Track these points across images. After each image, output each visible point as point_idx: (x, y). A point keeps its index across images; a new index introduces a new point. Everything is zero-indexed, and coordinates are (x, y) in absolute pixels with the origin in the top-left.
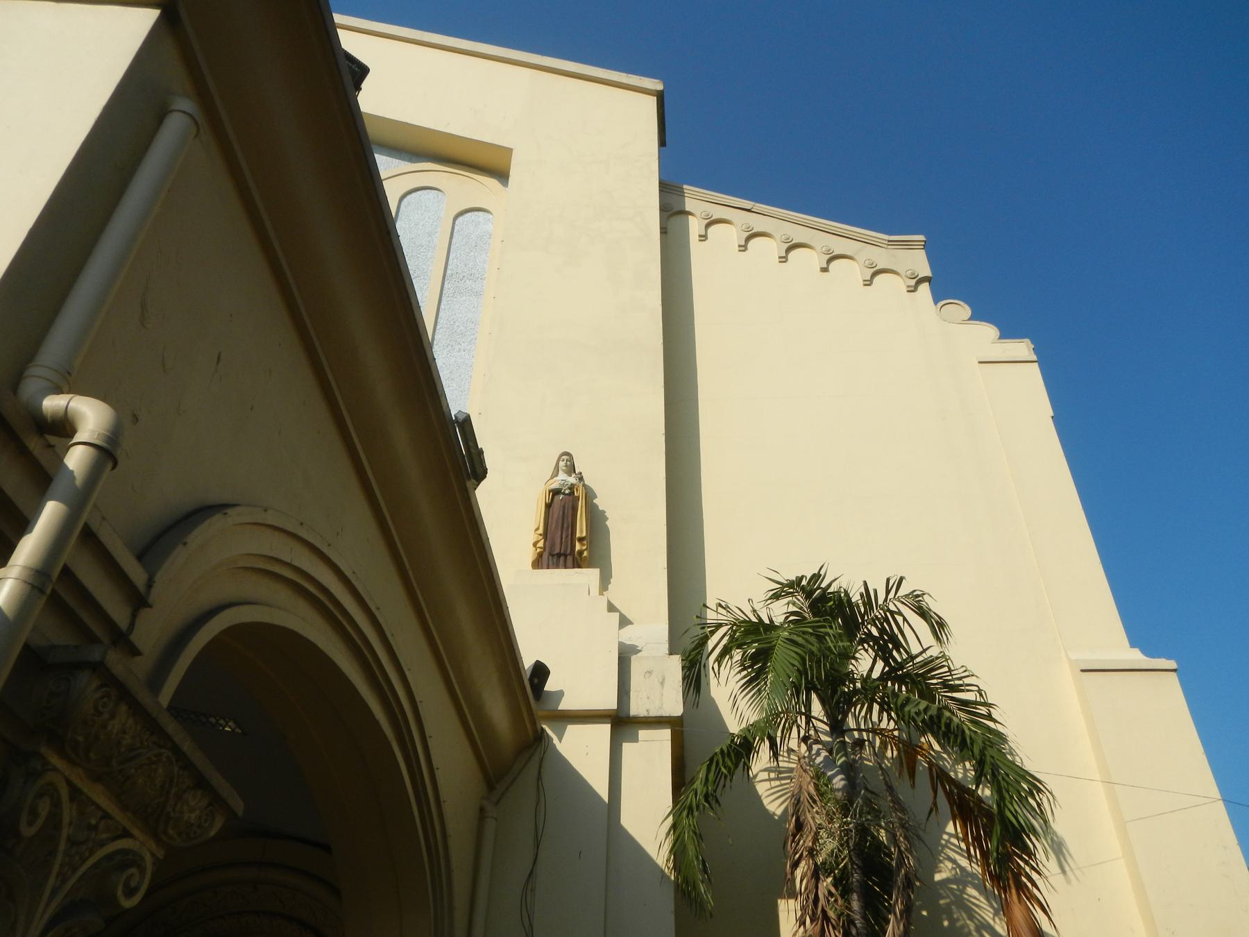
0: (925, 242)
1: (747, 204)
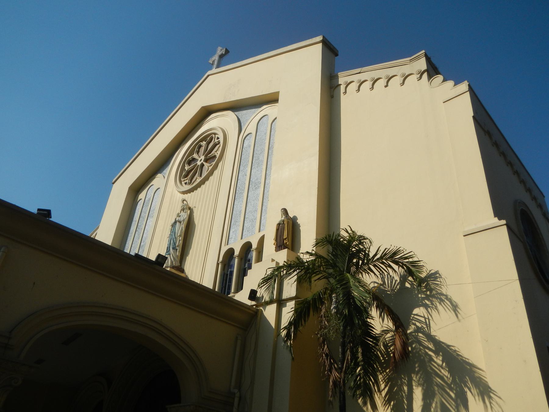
0: (425, 53)
1: (358, 70)
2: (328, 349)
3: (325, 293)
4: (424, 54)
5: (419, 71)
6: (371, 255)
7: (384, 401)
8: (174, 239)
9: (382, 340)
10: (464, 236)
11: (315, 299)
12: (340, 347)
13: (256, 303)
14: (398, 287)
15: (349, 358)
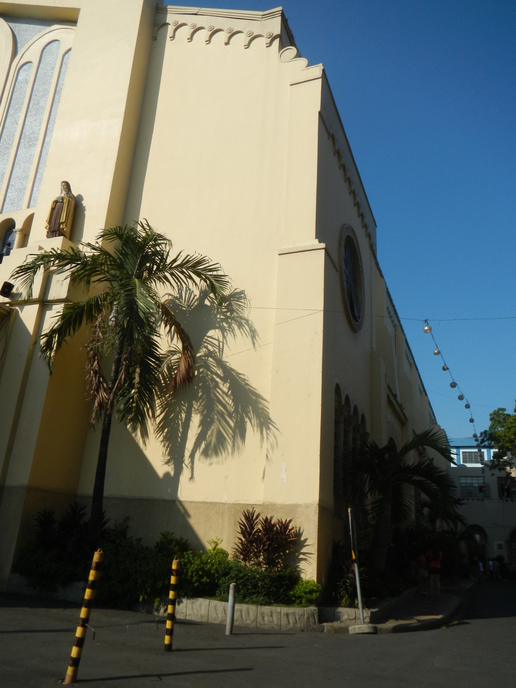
0: (282, 10)
1: (194, 10)
2: (99, 365)
3: (105, 299)
4: (281, 12)
5: (270, 35)
6: (169, 261)
7: (157, 428)
9: (167, 362)
10: (279, 255)
11: (91, 304)
12: (114, 365)
13: (10, 301)
14: (196, 304)
15: (123, 377)
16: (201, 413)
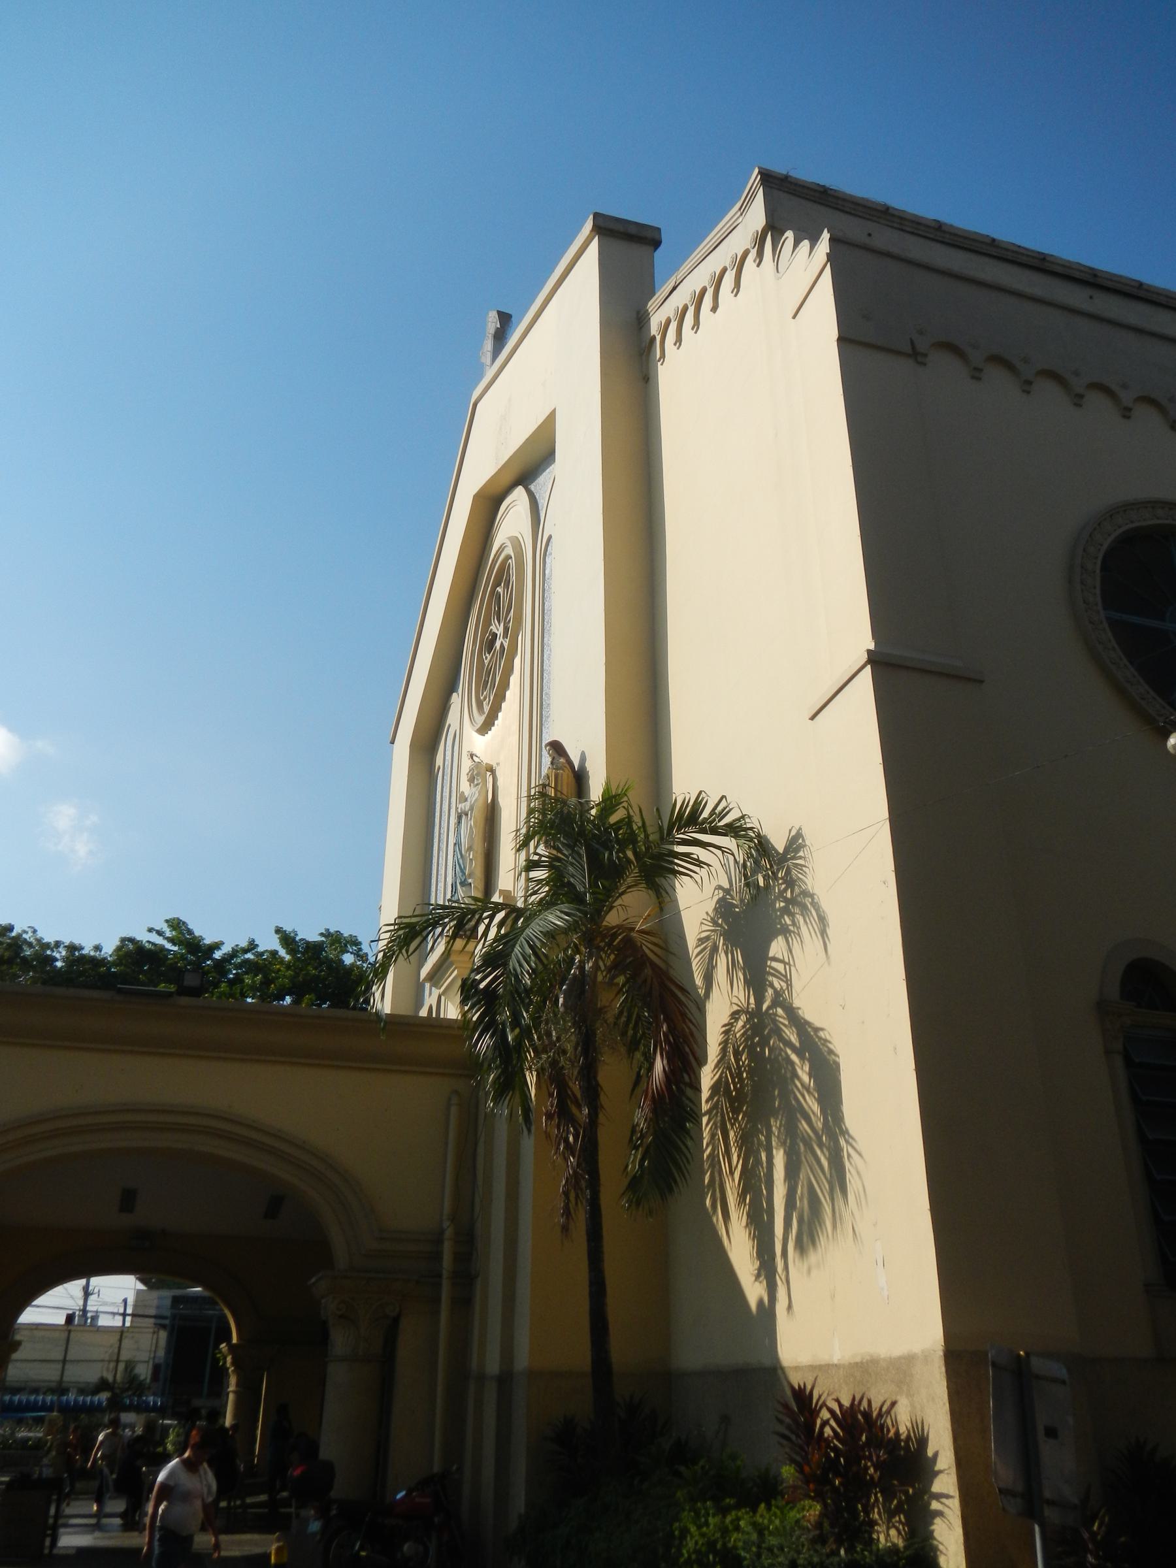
8: (461, 861)
16: (784, 1144)
